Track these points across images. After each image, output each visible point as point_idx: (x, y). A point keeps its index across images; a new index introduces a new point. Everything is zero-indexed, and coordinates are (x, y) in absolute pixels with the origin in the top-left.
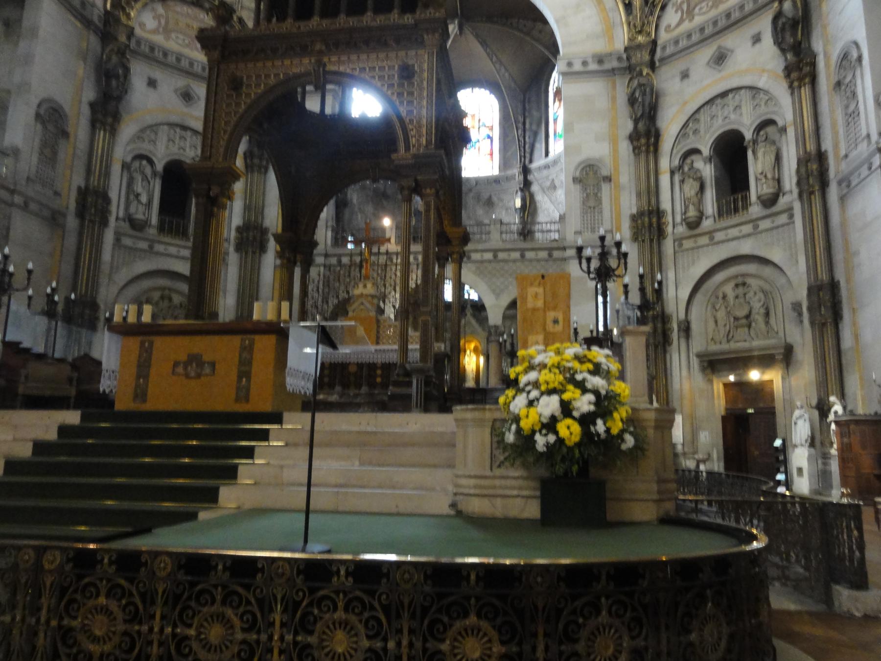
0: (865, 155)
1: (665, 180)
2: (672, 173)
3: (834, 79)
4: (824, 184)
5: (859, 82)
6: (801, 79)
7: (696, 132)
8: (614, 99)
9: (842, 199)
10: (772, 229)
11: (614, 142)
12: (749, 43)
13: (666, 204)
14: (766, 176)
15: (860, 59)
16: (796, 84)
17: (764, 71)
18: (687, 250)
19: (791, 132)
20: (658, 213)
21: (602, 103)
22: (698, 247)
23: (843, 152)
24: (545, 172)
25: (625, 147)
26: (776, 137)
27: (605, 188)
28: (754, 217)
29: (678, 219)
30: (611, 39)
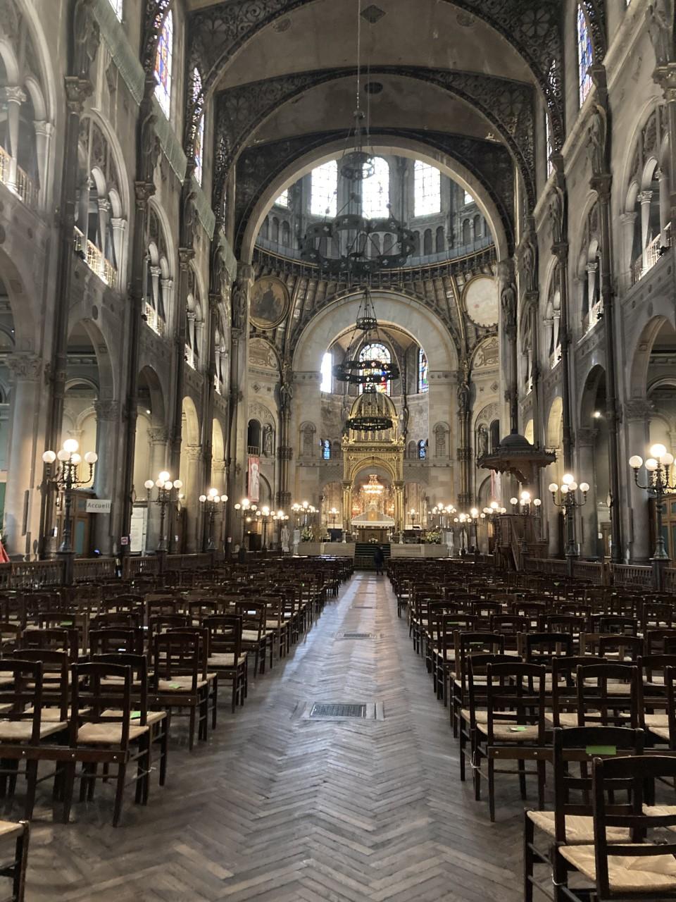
1: (473, 434)
7: (485, 416)
8: (451, 394)
11: (451, 414)
13: (473, 447)
20: (470, 449)
21: (446, 396)
24: (416, 402)
25: (455, 417)
27: (447, 435)
30: (451, 366)
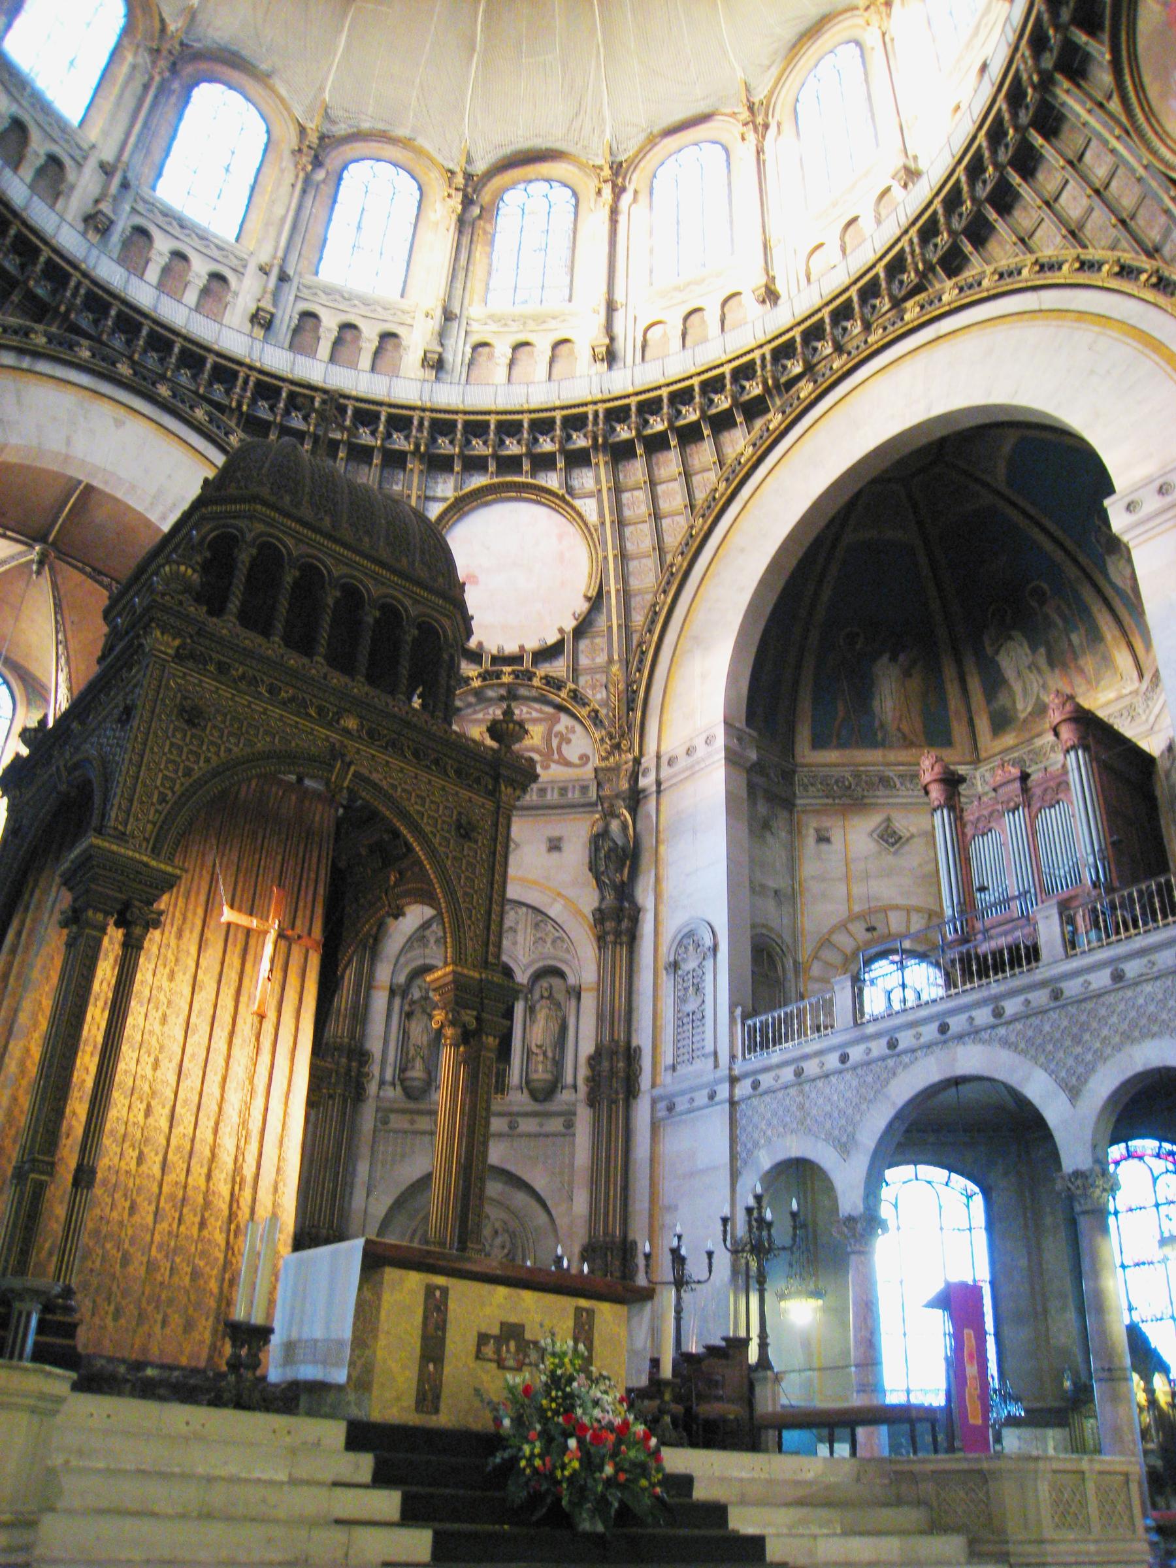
0: (709, 1077)
1: (379, 1001)
2: (392, 992)
3: (667, 955)
4: (631, 1090)
5: (709, 977)
6: (618, 934)
9: (655, 1127)
10: (537, 1136)
12: (544, 847)
13: (374, 1045)
14: (545, 1054)
15: (715, 949)
16: (610, 938)
17: (559, 894)
18: (396, 1132)
19: (589, 1002)
20: (361, 1056)
22: (416, 1133)
23: (669, 1060)
26: (560, 996)
28: (515, 1109)
29: (388, 1076)
